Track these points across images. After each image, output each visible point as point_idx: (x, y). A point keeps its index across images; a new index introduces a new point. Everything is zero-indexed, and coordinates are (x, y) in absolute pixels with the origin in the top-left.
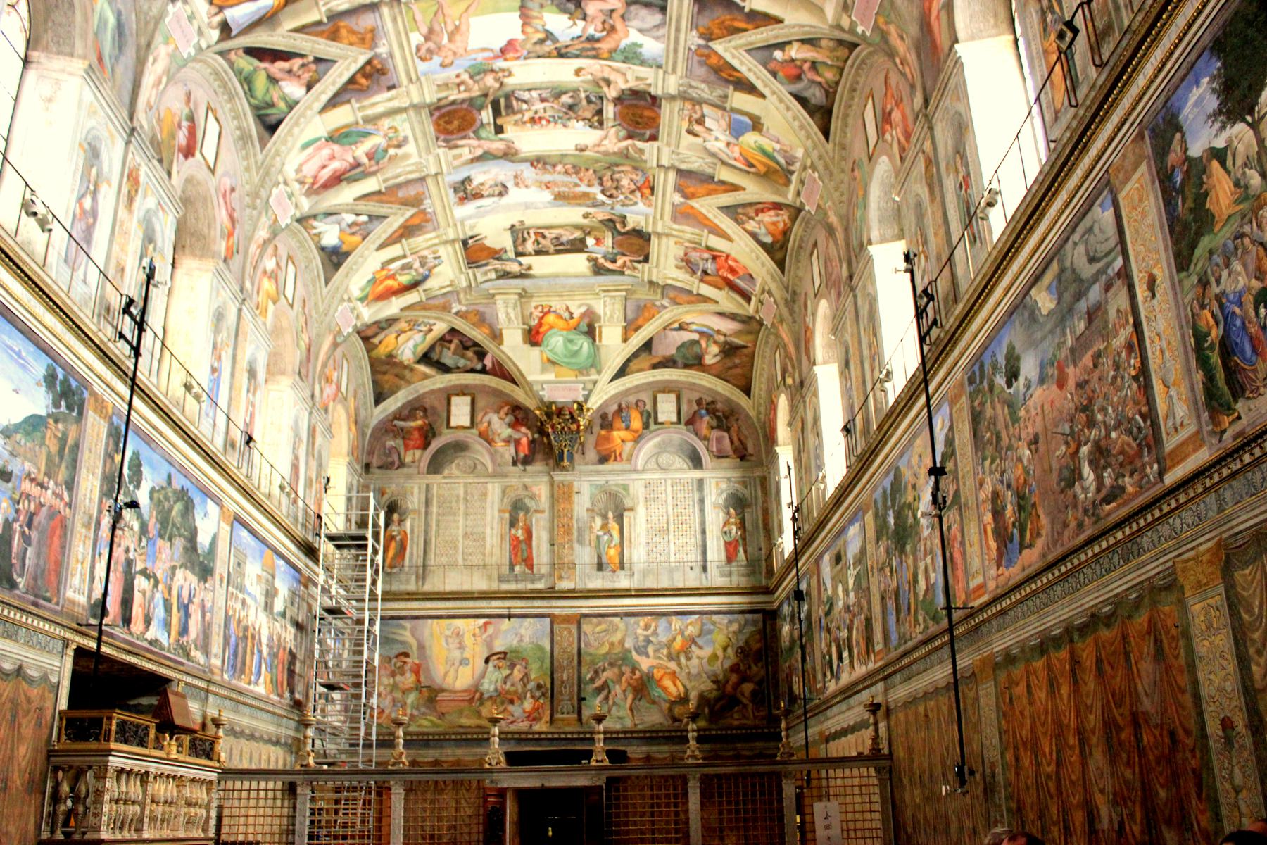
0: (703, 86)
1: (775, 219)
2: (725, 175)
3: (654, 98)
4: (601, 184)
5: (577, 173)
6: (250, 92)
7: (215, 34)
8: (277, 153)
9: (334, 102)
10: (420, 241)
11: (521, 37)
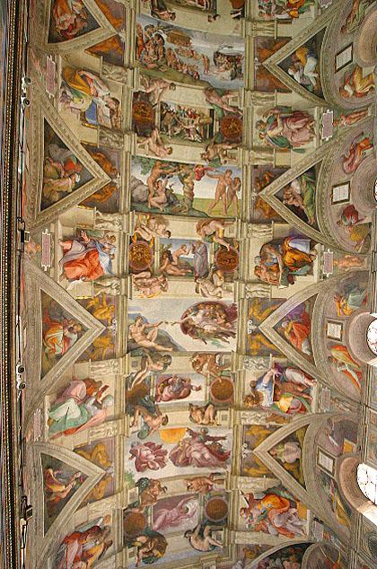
0: (112, 144)
1: (63, 18)
2: (96, 62)
3: (136, 132)
4: (164, 50)
5: (177, 63)
6: (313, 193)
7: (317, 246)
8: (316, 156)
9: (284, 169)
10: (265, 33)
11: (195, 181)
